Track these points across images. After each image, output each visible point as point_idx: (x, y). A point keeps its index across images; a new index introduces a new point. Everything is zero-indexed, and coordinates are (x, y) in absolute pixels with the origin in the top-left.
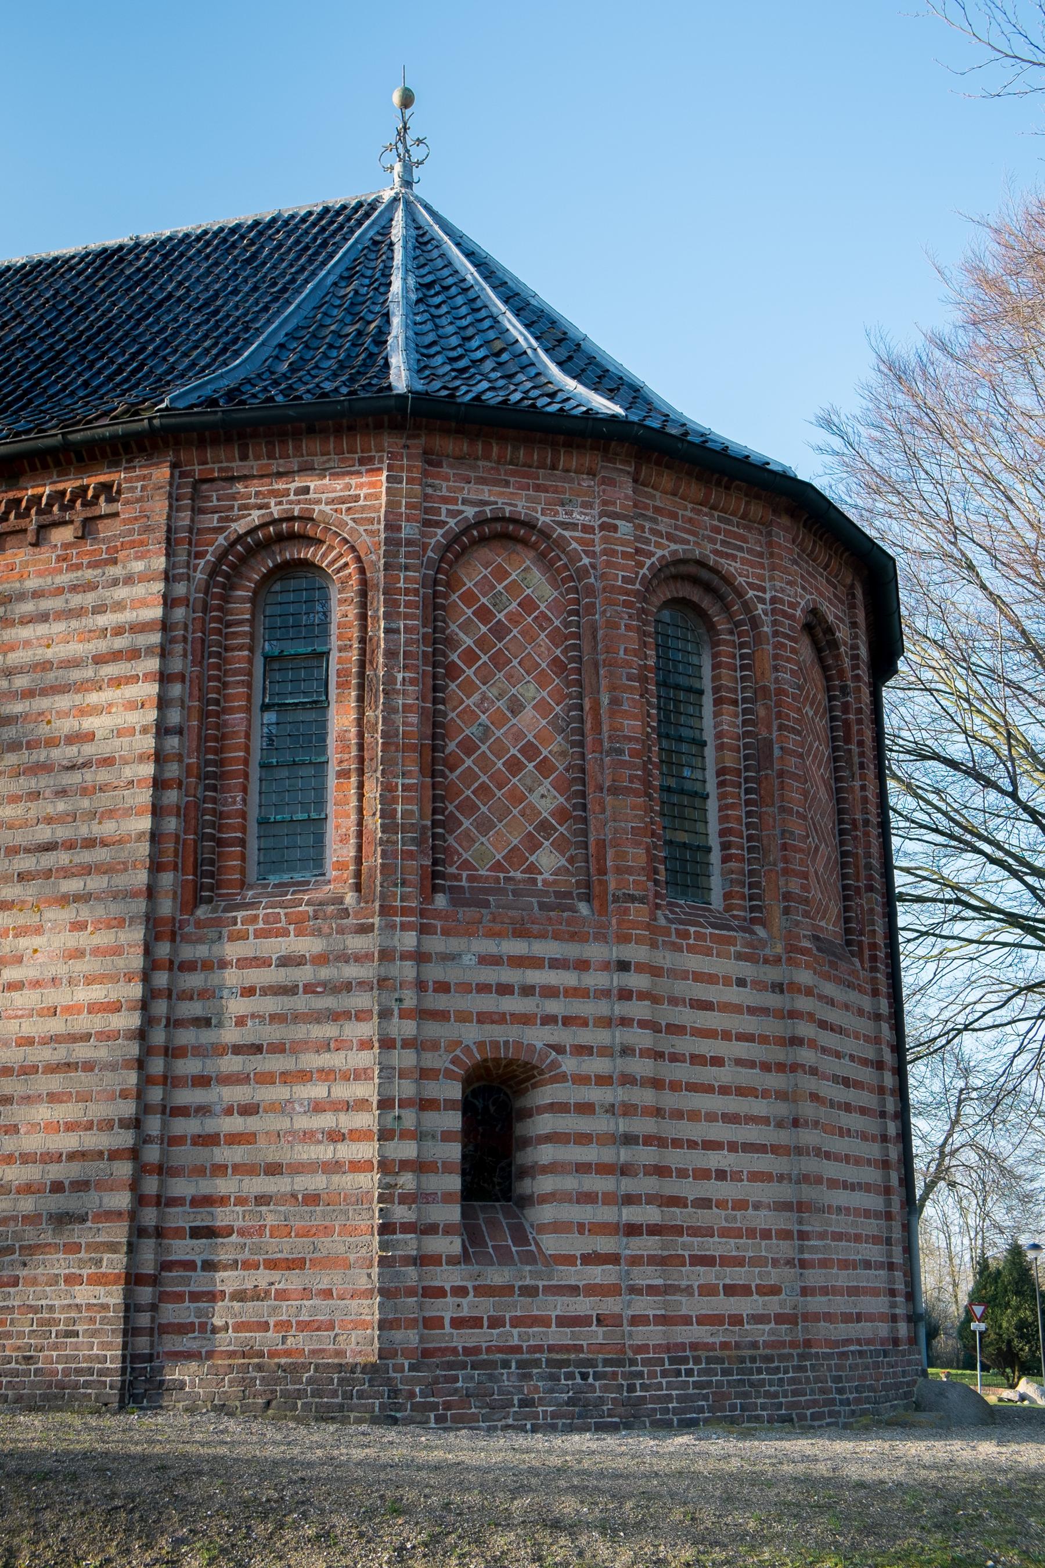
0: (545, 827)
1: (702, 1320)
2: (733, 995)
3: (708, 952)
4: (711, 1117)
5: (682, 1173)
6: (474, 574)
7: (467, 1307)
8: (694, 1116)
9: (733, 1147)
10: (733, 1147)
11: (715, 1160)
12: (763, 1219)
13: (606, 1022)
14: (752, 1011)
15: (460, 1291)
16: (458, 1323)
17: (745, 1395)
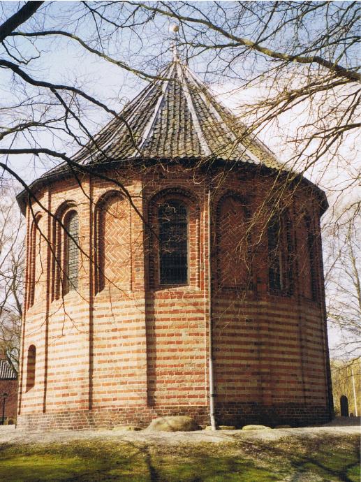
17: (59, 422)
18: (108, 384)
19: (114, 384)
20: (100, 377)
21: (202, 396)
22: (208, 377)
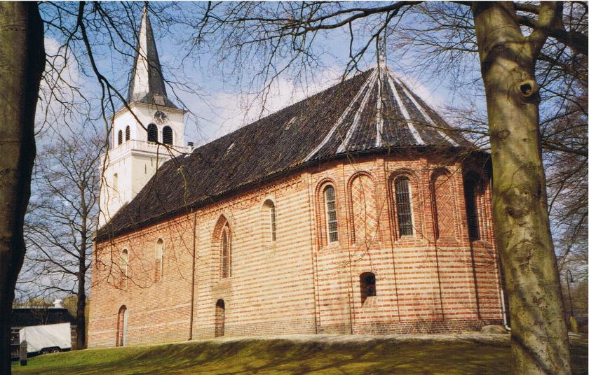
0: (373, 228)
1: (409, 316)
2: (415, 254)
3: (407, 247)
4: (410, 278)
5: (403, 289)
6: (357, 181)
7: (363, 315)
8: (405, 279)
9: (416, 283)
10: (416, 283)
11: (411, 286)
12: (424, 296)
13: (384, 264)
14: (419, 257)
15: (362, 313)
16: (362, 318)
18: (452, 303)
19: (456, 303)
20: (446, 298)
21: (499, 313)
22: (501, 300)
